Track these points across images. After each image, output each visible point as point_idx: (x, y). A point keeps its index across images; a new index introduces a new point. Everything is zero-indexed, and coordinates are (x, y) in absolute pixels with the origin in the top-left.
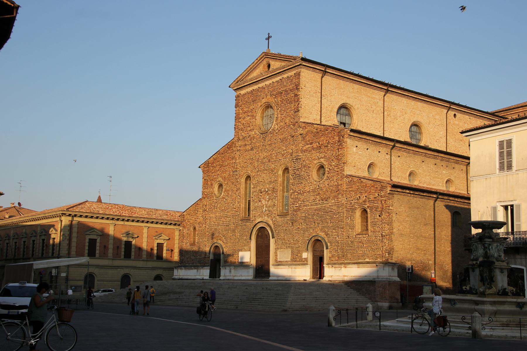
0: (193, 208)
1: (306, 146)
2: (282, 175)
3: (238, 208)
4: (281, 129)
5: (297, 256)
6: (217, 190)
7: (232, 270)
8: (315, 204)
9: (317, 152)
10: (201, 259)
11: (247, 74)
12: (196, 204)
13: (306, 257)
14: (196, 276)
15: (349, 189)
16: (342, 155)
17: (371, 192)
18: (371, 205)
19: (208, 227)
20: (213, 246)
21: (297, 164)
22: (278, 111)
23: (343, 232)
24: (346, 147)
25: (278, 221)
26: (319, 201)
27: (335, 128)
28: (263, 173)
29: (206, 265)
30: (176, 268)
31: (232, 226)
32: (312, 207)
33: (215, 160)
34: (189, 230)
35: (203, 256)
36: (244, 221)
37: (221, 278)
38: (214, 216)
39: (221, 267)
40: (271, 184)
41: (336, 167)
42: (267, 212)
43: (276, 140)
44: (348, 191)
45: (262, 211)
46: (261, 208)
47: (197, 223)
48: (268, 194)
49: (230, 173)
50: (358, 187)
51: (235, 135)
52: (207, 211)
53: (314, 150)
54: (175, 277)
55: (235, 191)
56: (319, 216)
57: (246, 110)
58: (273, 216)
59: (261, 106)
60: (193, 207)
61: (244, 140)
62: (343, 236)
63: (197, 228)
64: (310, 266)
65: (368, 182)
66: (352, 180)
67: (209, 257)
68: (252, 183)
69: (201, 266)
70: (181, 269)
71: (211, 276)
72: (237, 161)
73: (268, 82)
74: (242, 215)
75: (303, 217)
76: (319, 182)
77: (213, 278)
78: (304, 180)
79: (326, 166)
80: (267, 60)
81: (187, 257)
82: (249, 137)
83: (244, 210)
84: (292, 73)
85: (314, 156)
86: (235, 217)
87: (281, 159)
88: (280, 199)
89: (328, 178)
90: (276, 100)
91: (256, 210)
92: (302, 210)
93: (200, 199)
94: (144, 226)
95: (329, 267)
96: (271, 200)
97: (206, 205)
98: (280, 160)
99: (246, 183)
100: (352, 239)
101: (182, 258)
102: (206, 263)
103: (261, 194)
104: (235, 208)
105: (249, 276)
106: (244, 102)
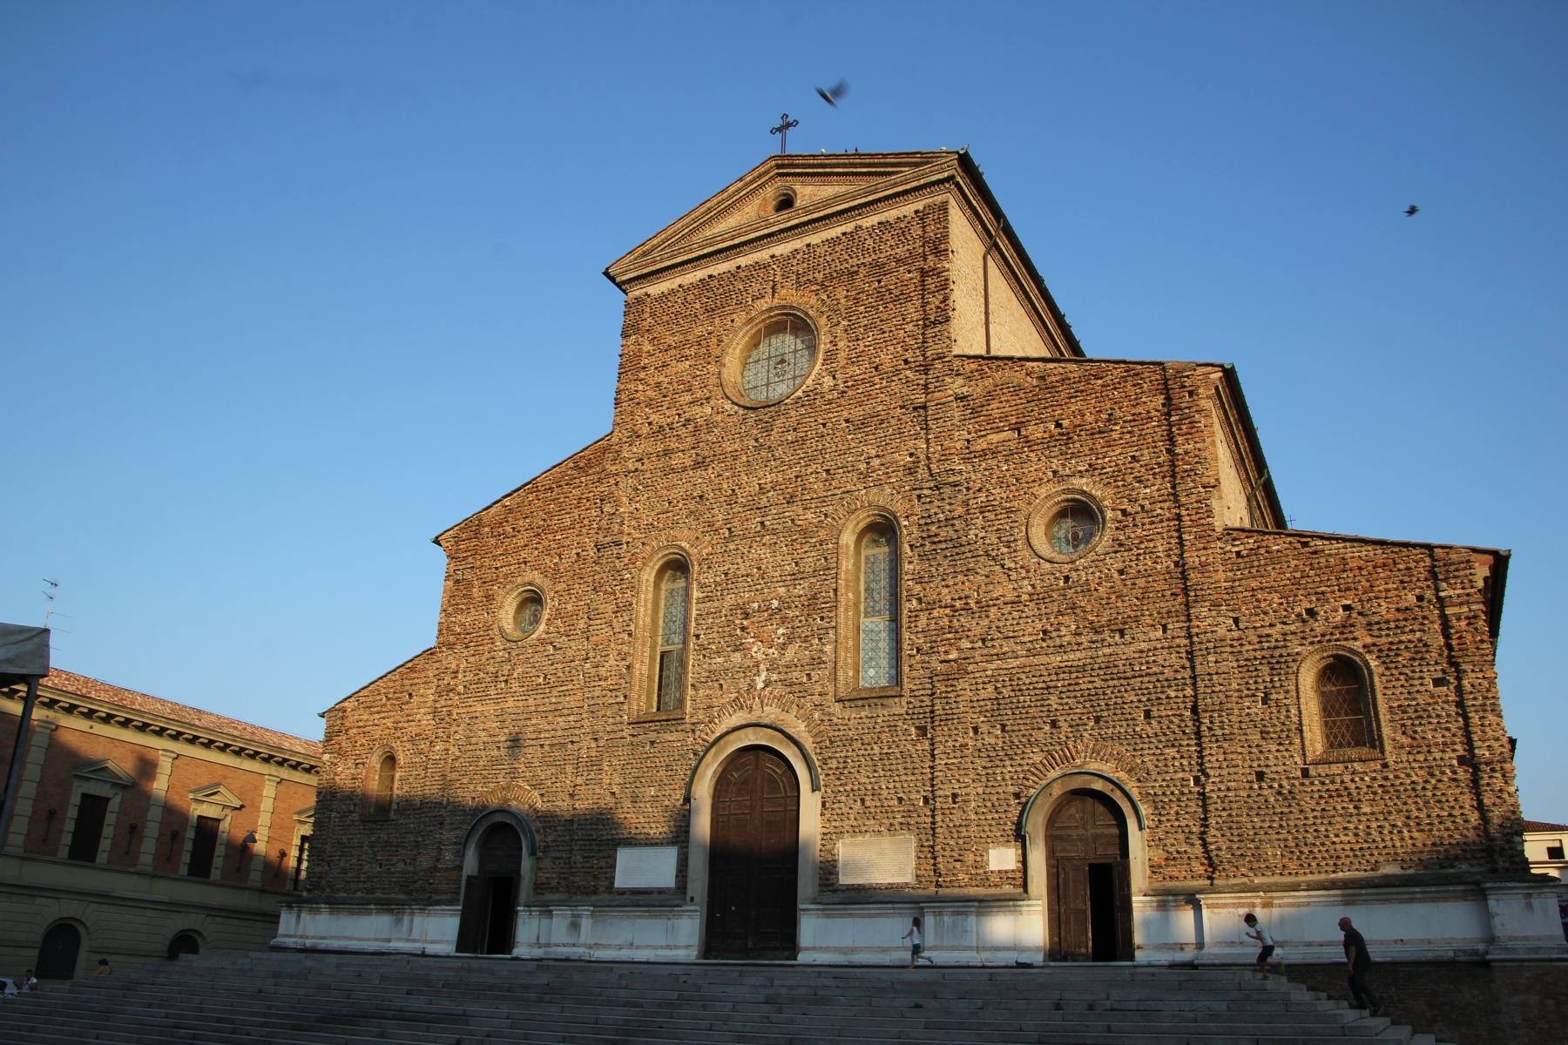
0: (391, 684)
1: (990, 437)
2: (852, 548)
3: (621, 676)
4: (853, 386)
6: (511, 616)
8: (1051, 650)
9: (1053, 454)
10: (415, 873)
11: (687, 230)
12: (409, 668)
14: (389, 941)
15: (1244, 582)
16: (1196, 456)
17: (1376, 589)
18: (1384, 640)
19: (458, 753)
21: (937, 503)
22: (839, 330)
23: (1234, 756)
24: (1208, 428)
25: (835, 720)
26: (1080, 634)
27: (1139, 367)
28: (754, 545)
29: (435, 897)
30: (290, 908)
31: (587, 747)
32: (1035, 661)
33: (511, 511)
34: (361, 766)
35: (425, 865)
36: (647, 725)
37: (519, 951)
38: (490, 708)
39: (519, 908)
40: (802, 582)
41: (1159, 505)
42: (779, 690)
43: (824, 425)
44: (1240, 589)
45: (752, 686)
46: (742, 675)
47: (405, 739)
48: (784, 620)
49: (584, 553)
50: (1298, 575)
51: (616, 424)
52: (459, 694)
53: (1035, 448)
54: (283, 940)
55: (611, 614)
56: (1079, 694)
57: (670, 340)
58: (809, 705)
59: (751, 320)
60: (390, 680)
61: (661, 437)
62: (1232, 770)
63: (402, 759)
65: (1355, 550)
66: (1259, 547)
67: (460, 868)
68: (699, 583)
69: (417, 901)
70: (318, 911)
71: (463, 943)
72: (622, 510)
73: (782, 249)
74: (642, 701)
75: (982, 703)
76: (1073, 562)
77: (474, 951)
78: (982, 559)
79: (1106, 503)
80: (779, 183)
81: (342, 864)
82: (684, 425)
83: (645, 685)
84: (908, 209)
85: (1032, 469)
86: (600, 714)
87: (854, 488)
88: (846, 638)
89: (1121, 545)
90: (825, 297)
91: (716, 684)
92: (977, 675)
93: (430, 652)
94: (163, 750)
96: (798, 640)
97: (457, 672)
98: (848, 492)
99: (657, 586)
100: (1285, 783)
101: (318, 869)
102: (436, 892)
103: (745, 622)
104: (606, 679)
105: (677, 947)
106: (665, 318)
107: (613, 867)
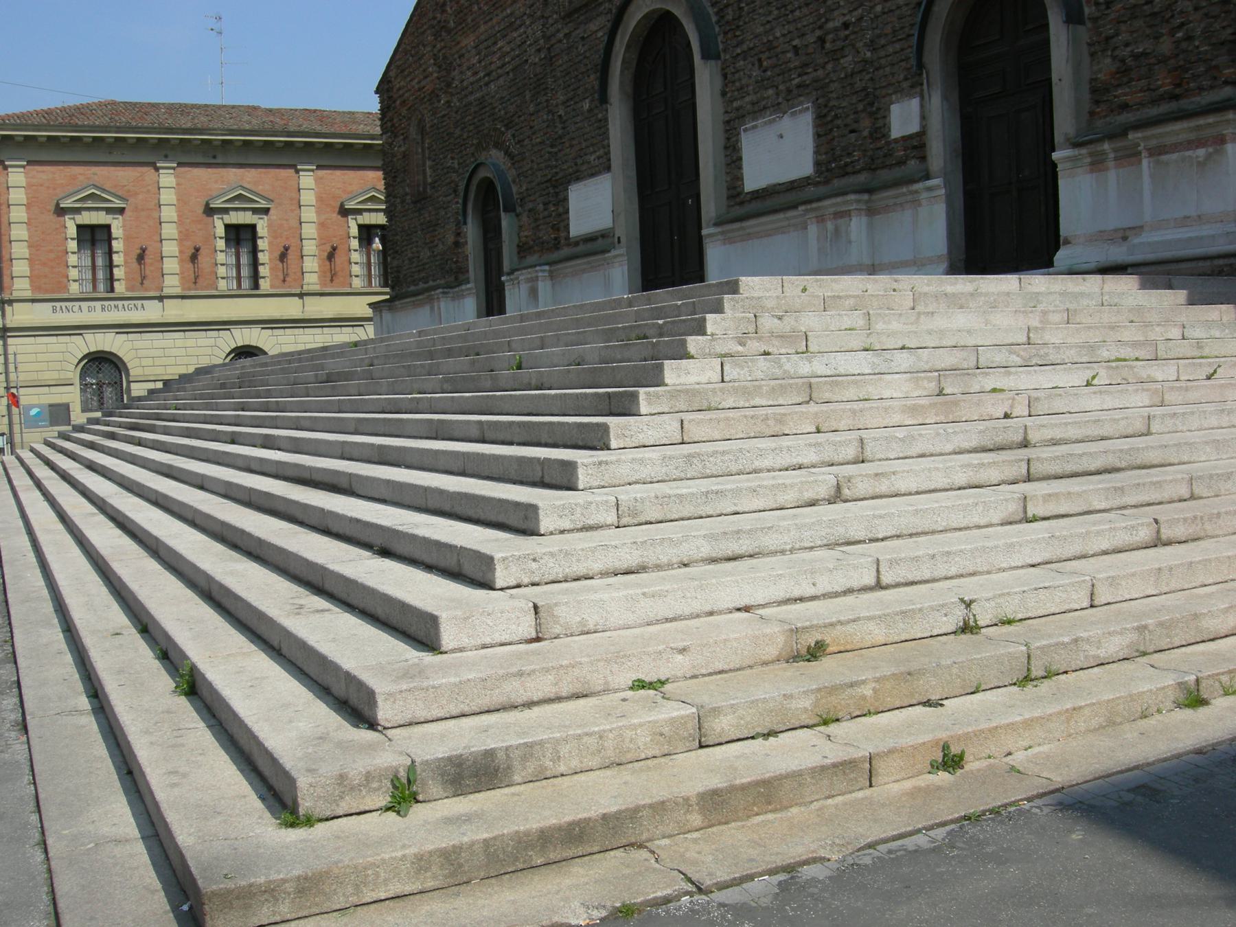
5: (852, 131)
7: (541, 285)
13: (914, 128)
20: (473, 188)
39: (503, 278)
64: (947, 184)
95: (1097, 164)
107: (567, 212)
